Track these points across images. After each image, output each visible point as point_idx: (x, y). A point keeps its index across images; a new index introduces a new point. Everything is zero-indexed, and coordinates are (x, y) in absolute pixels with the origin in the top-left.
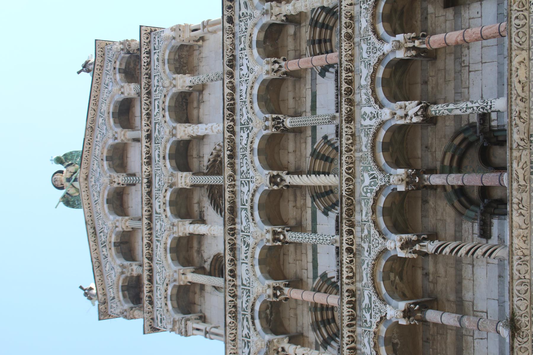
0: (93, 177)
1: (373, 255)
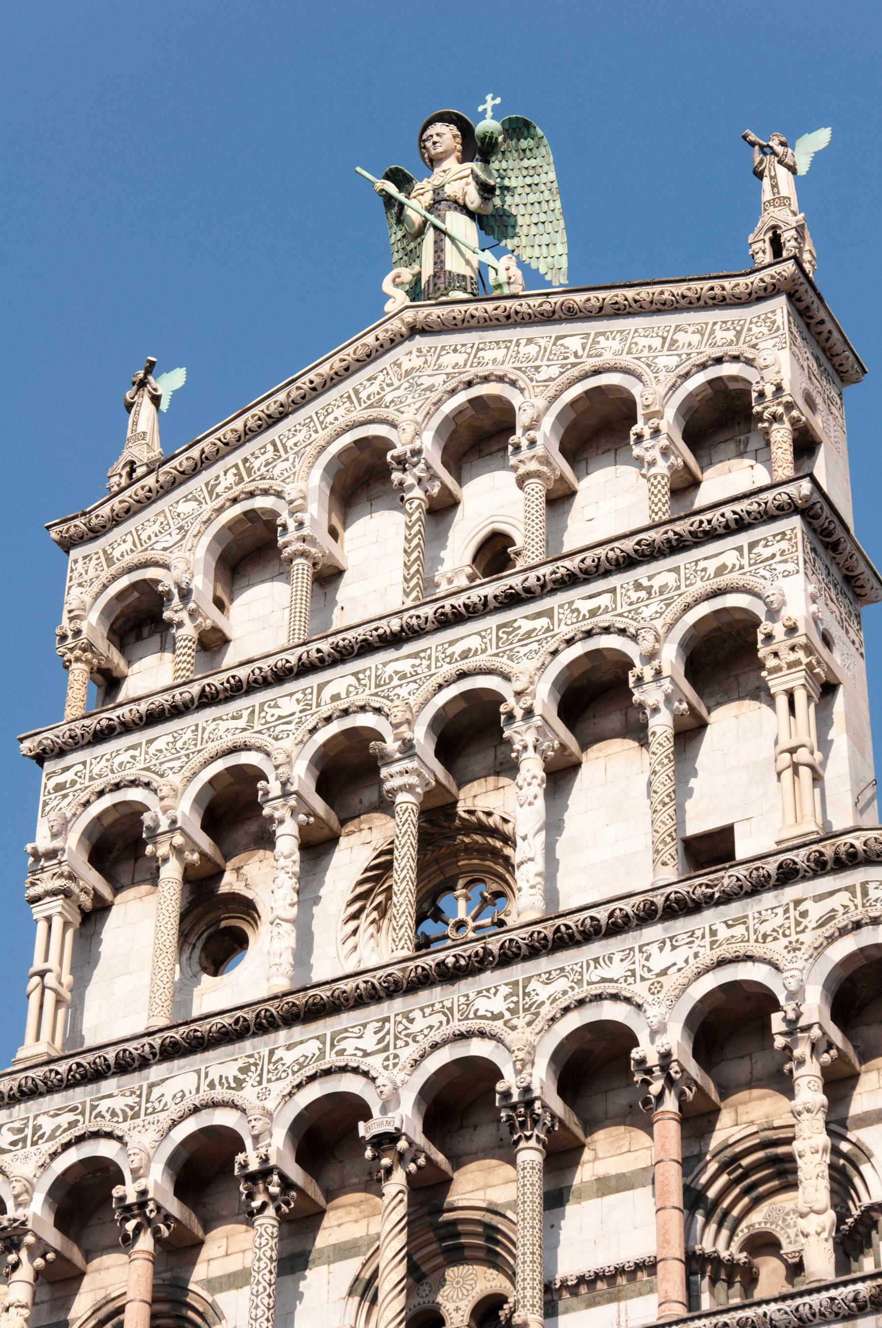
0: (423, 359)
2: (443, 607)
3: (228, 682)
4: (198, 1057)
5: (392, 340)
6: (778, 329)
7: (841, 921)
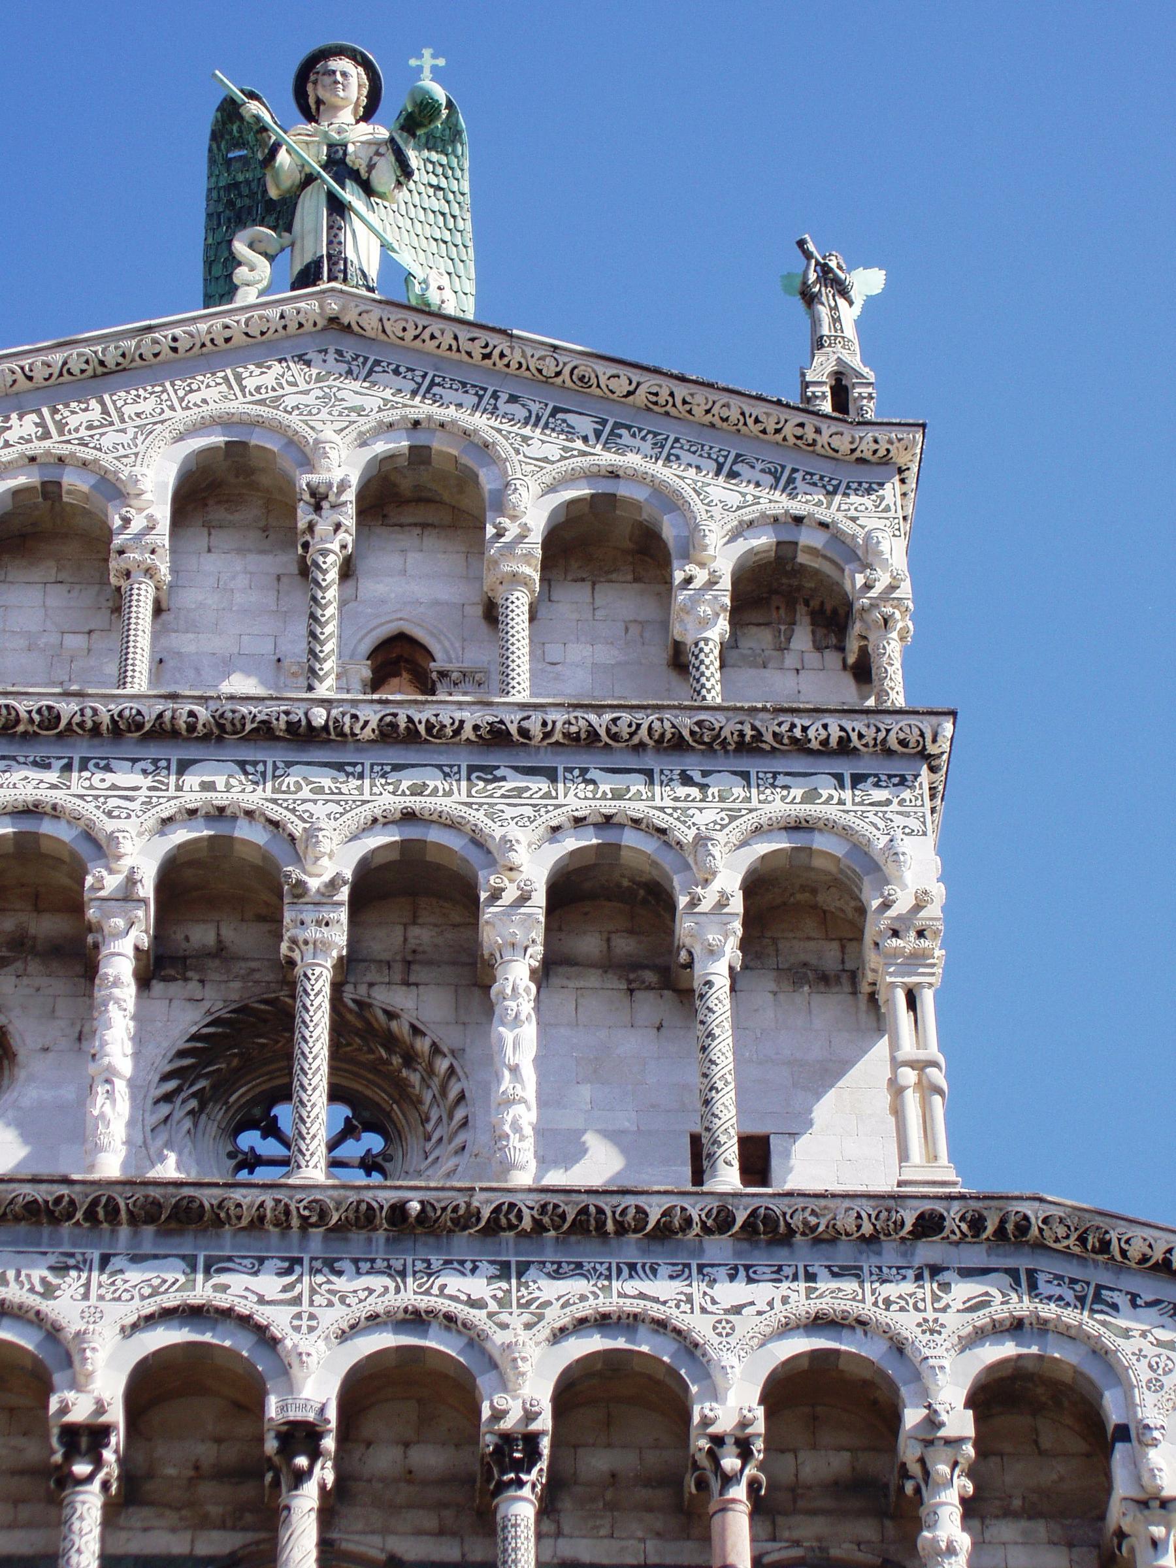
2: (395, 715)
3: (39, 711)
5: (301, 325)
6: (887, 509)
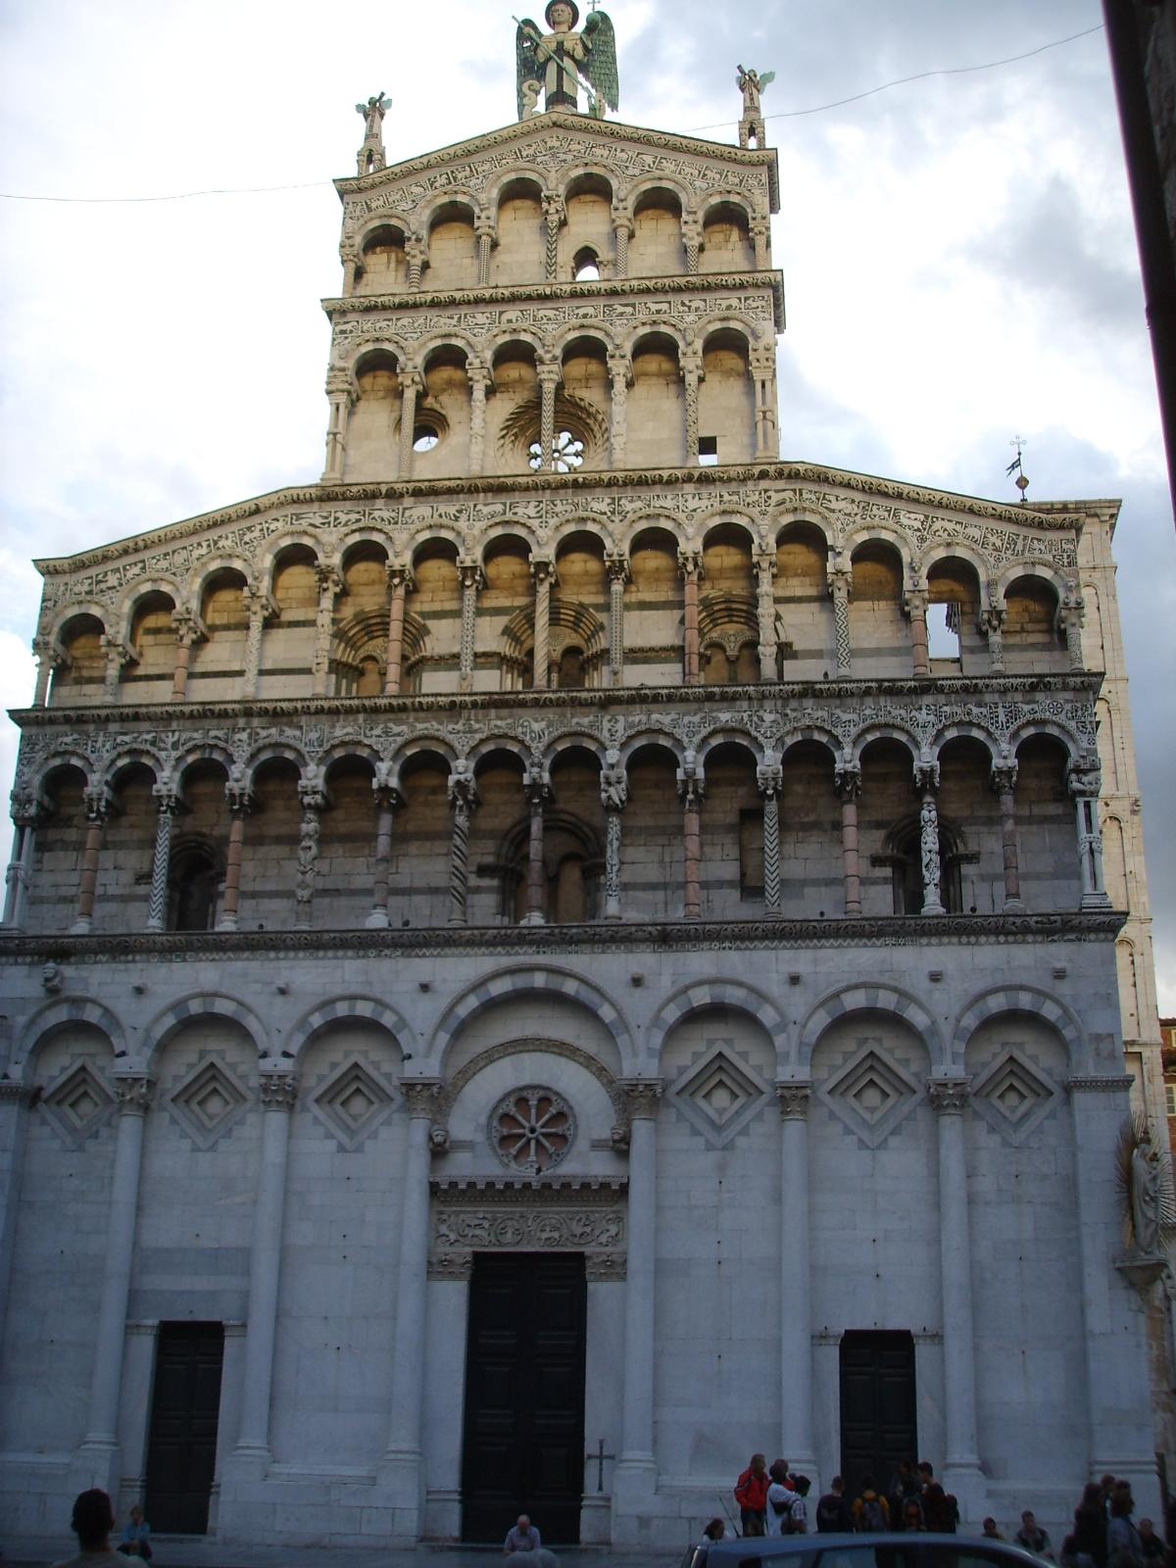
1: (450, 738)
4: (432, 498)
7: (788, 505)
